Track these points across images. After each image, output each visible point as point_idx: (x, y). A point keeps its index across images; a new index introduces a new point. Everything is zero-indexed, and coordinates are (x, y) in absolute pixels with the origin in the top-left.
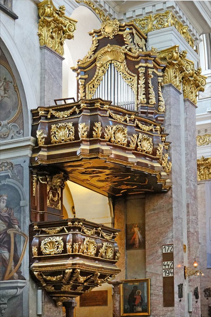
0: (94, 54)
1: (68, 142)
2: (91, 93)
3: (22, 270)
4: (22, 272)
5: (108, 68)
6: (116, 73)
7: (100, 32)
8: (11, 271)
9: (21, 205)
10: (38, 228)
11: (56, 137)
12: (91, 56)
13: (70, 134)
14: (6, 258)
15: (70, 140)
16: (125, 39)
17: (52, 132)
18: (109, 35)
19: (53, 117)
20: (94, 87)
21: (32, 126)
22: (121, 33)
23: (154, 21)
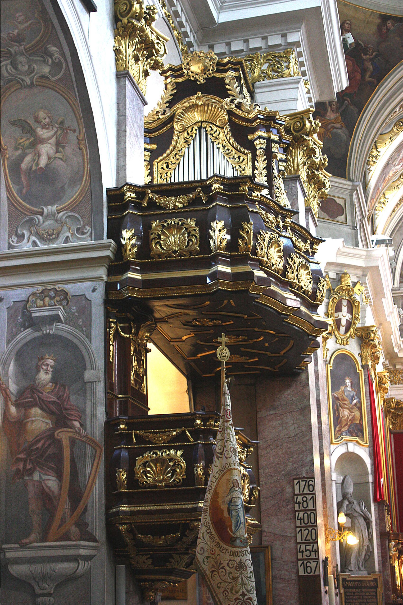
0: (170, 107)
1: (185, 256)
2: (163, 177)
3: (88, 518)
4: (90, 524)
5: (196, 134)
6: (210, 145)
7: (181, 69)
8: (63, 522)
9: (85, 380)
10: (128, 430)
11: (161, 245)
12: (165, 111)
13: (192, 241)
14: (53, 492)
15: (191, 253)
16: (227, 87)
17: (152, 234)
18: (197, 76)
19: (152, 204)
20: (168, 167)
21: (108, 220)
22: (220, 76)
23: (264, 64)
